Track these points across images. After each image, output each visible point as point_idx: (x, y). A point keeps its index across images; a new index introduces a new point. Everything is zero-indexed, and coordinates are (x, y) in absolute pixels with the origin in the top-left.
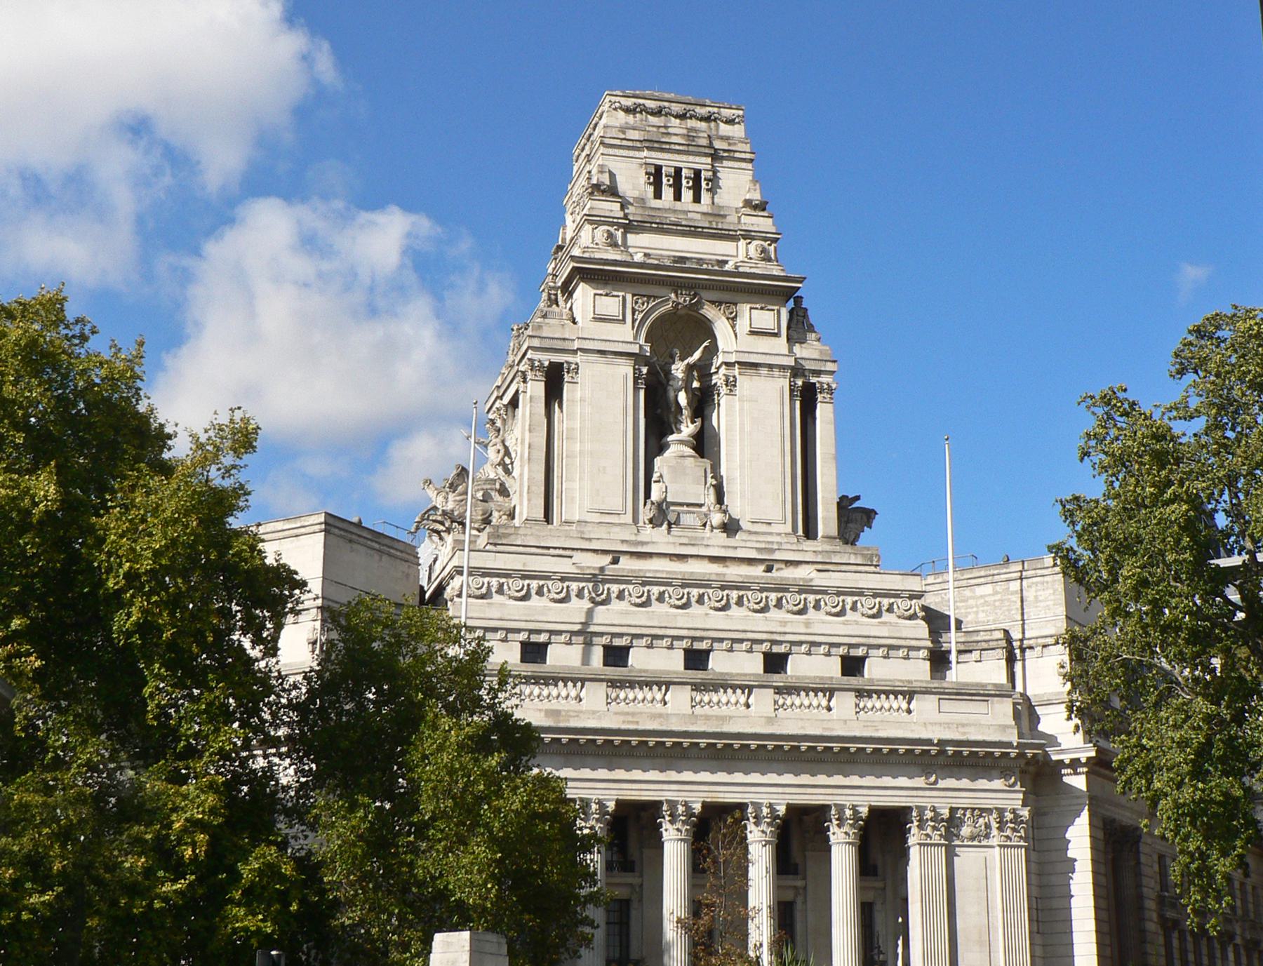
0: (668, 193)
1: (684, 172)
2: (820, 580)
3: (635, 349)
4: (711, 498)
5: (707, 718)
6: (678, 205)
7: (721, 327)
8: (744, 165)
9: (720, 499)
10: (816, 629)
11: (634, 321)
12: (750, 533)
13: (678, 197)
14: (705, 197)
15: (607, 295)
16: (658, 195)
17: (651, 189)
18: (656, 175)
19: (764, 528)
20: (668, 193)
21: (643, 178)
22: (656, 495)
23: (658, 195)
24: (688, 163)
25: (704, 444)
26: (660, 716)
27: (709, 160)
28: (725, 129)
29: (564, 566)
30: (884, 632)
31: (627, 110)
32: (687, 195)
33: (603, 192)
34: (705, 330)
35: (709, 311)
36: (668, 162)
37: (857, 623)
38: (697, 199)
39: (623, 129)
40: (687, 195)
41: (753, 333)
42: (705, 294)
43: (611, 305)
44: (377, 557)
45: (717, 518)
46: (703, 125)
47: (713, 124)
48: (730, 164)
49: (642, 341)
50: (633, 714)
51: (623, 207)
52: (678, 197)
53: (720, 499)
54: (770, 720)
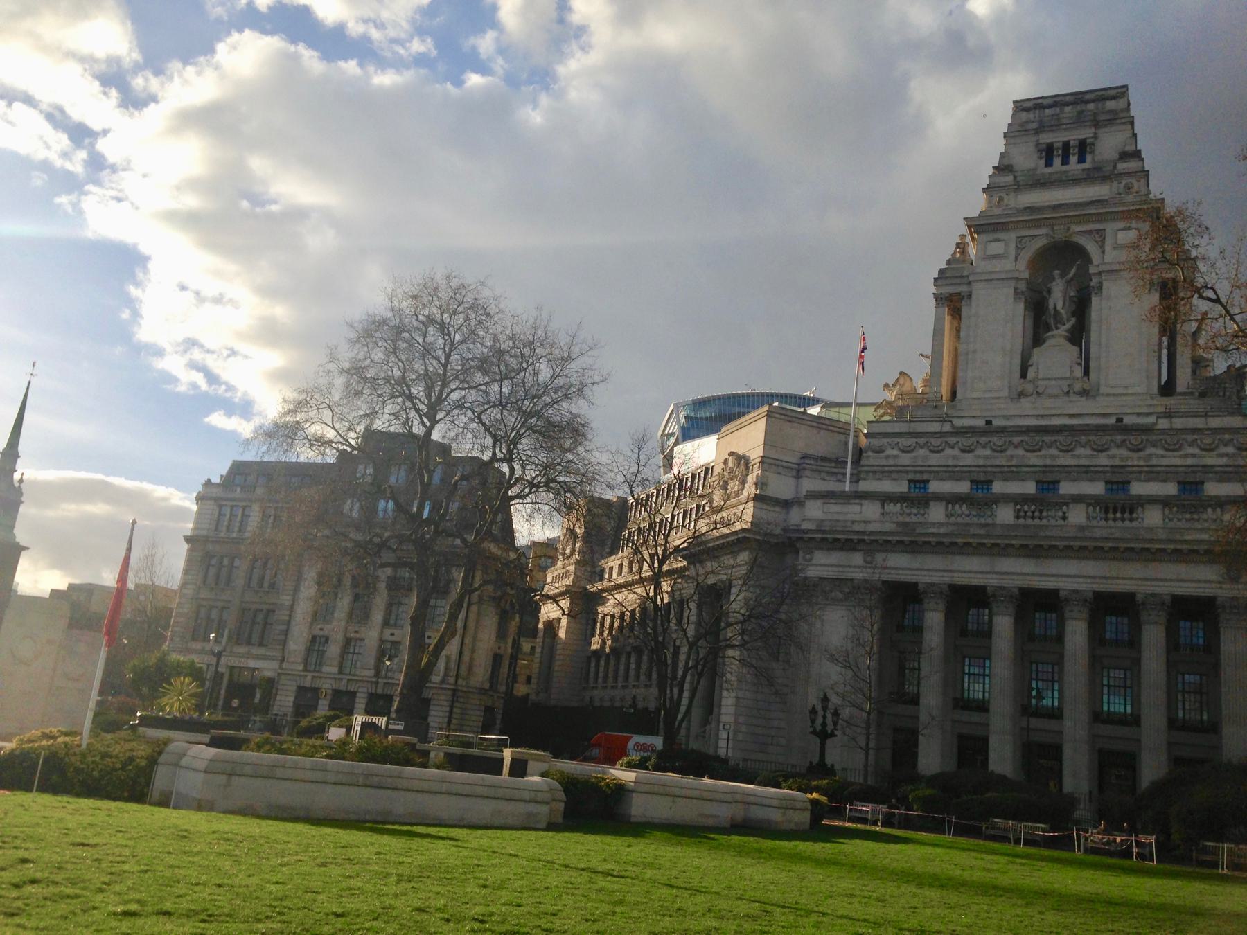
0: (1057, 161)
1: (1072, 143)
2: (1163, 424)
3: (1016, 275)
4: (1079, 372)
5: (1026, 527)
6: (1065, 168)
7: (1091, 248)
8: (1124, 127)
9: (1086, 372)
10: (1154, 462)
11: (1016, 258)
12: (1108, 395)
13: (1065, 161)
14: (1089, 158)
15: (997, 240)
16: (1049, 163)
17: (1043, 161)
18: (1048, 153)
19: (1121, 391)
20: (1057, 161)
21: (1035, 156)
22: (1031, 373)
23: (1049, 163)
24: (1074, 136)
25: (1078, 335)
26: (987, 525)
27: (1093, 130)
28: (1111, 105)
29: (947, 428)
30: (1224, 461)
31: (1027, 110)
32: (1073, 159)
33: (1003, 170)
34: (1080, 254)
35: (1082, 240)
36: (1056, 138)
37: (1194, 456)
38: (1082, 160)
39: (1022, 125)
40: (1073, 159)
41: (1118, 247)
42: (1076, 228)
43: (996, 248)
44: (815, 431)
45: (1078, 387)
46: (1091, 106)
47: (1100, 105)
48: (1113, 128)
49: (1022, 266)
50: (967, 524)
51: (1015, 177)
52: (1065, 161)
53: (1086, 372)
54: (1082, 528)
